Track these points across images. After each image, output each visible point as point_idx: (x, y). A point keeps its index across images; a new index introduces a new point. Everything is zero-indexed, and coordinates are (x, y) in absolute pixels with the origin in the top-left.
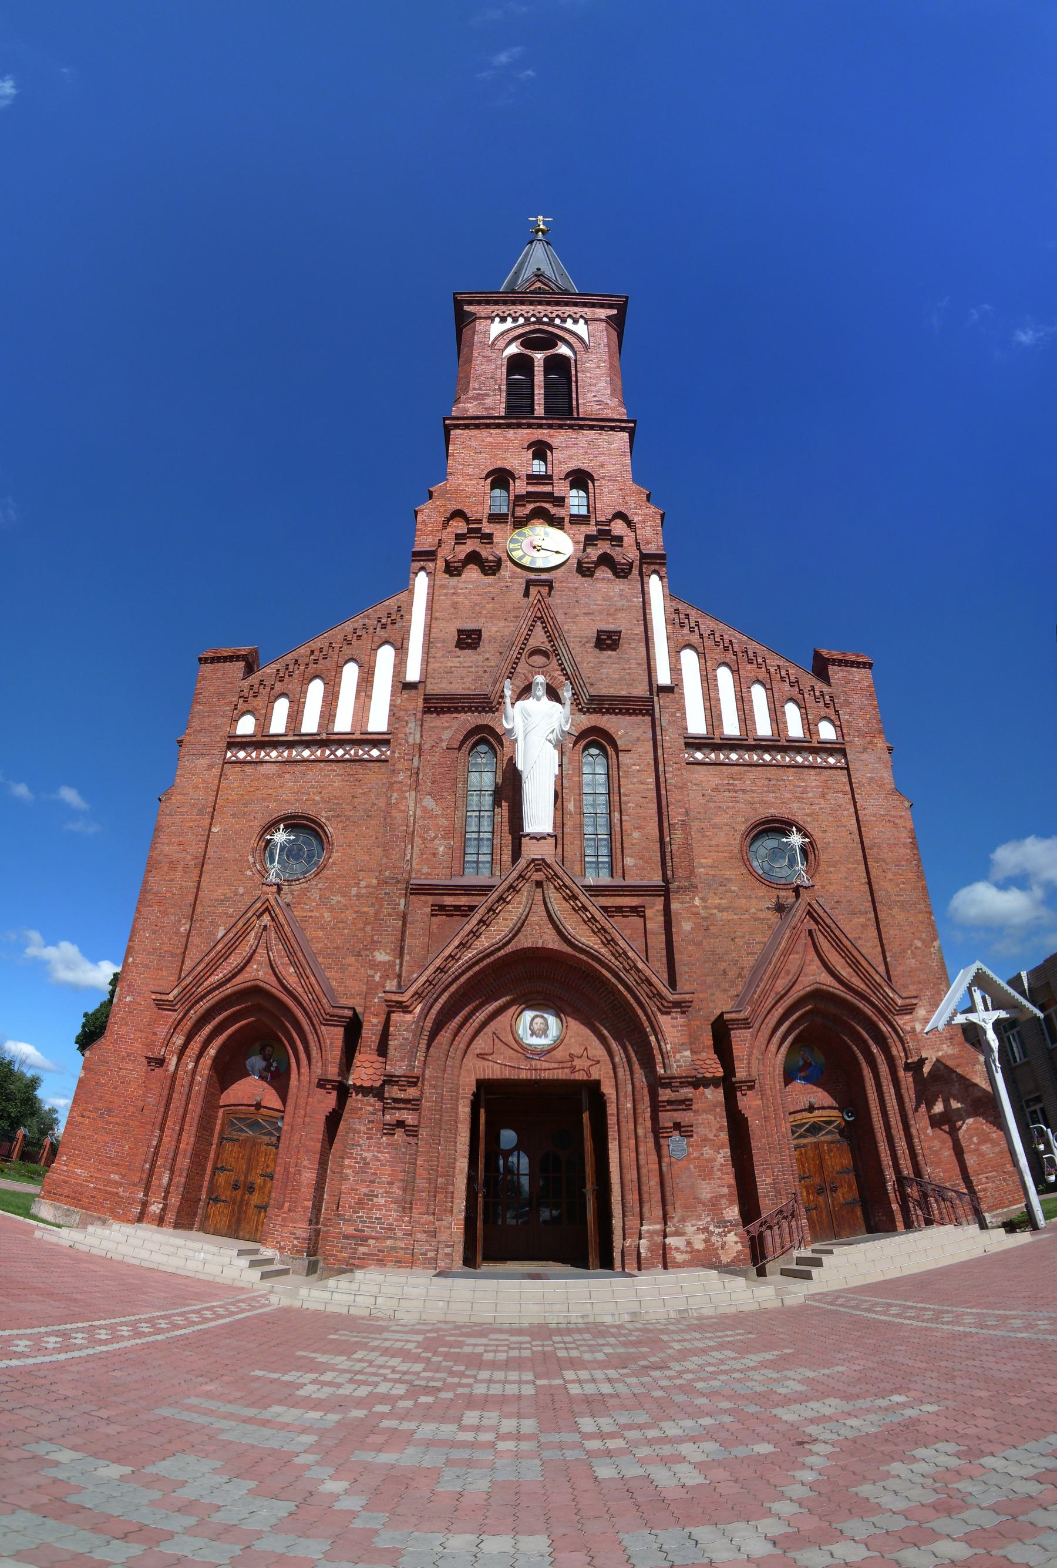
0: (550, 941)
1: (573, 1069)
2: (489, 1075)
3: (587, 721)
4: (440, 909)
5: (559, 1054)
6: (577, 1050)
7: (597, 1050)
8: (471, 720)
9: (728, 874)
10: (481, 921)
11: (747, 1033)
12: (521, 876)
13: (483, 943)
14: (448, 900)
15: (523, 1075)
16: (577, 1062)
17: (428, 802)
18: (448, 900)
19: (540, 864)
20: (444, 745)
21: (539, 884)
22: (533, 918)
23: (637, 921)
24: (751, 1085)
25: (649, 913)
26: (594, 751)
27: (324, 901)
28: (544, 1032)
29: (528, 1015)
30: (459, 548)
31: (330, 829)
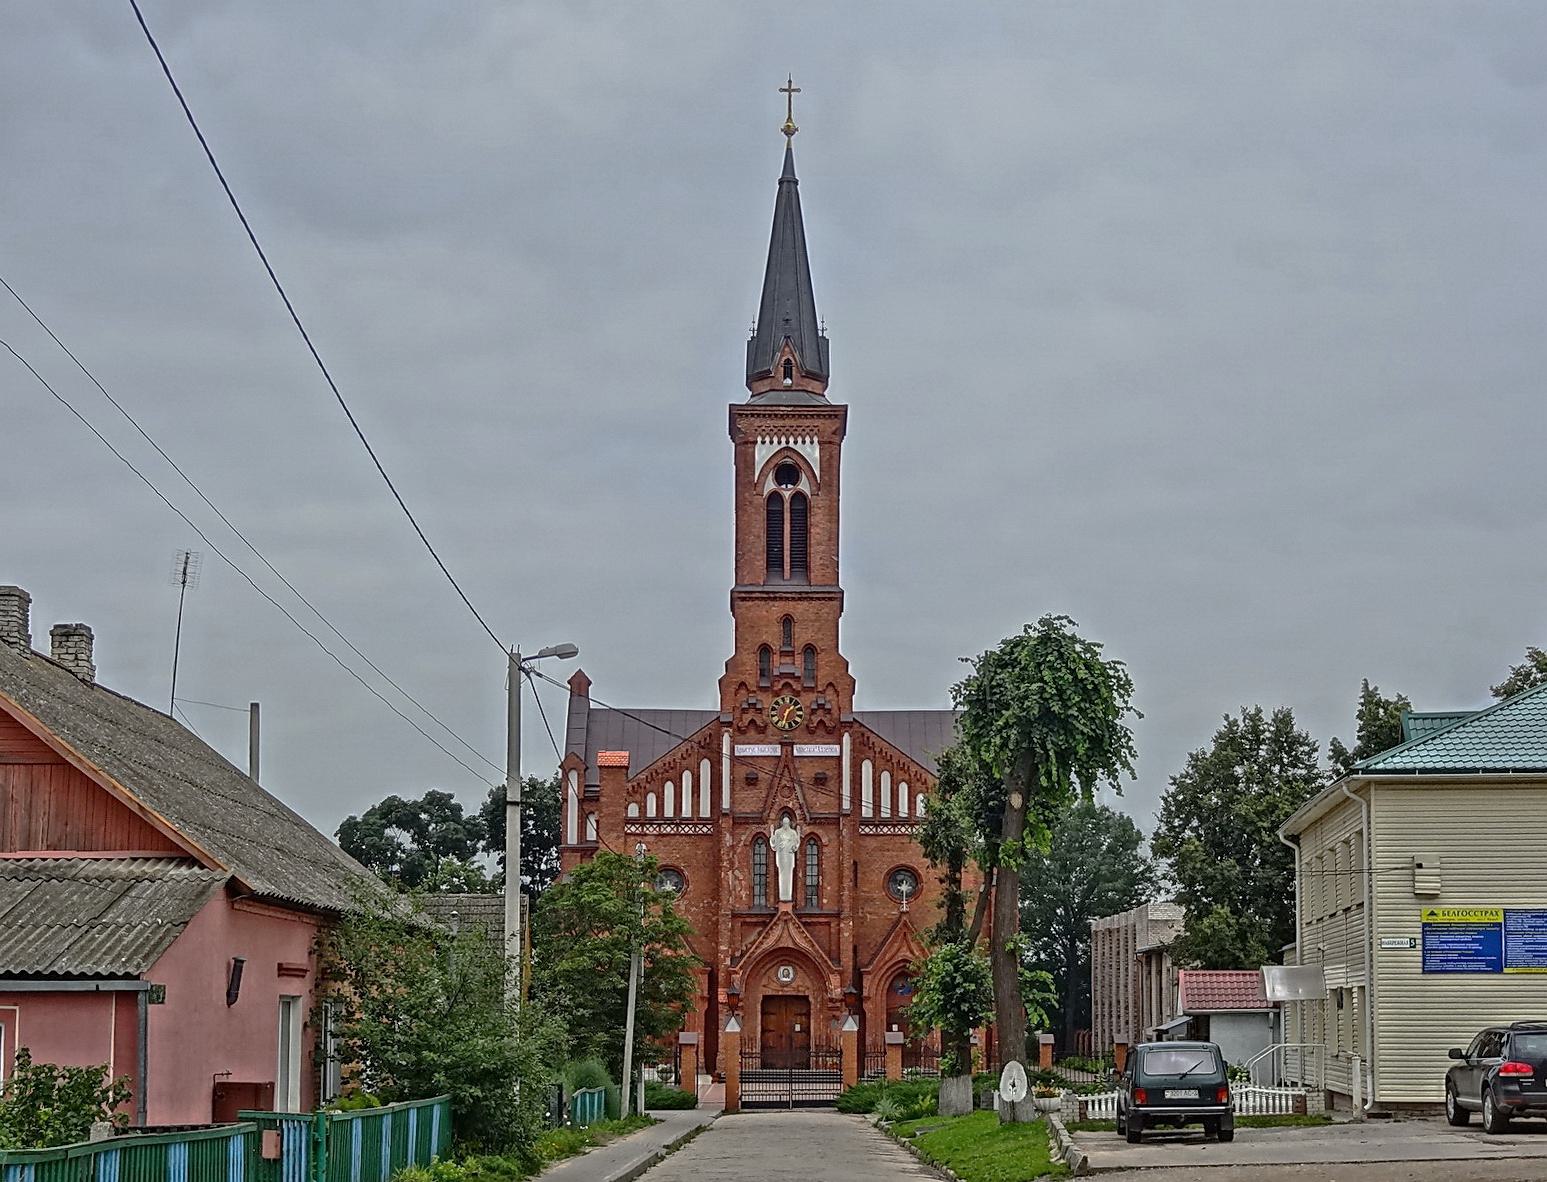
0: (791, 946)
1: (799, 991)
2: (767, 994)
3: (808, 829)
4: (744, 924)
5: (793, 984)
6: (801, 984)
7: (808, 984)
8: (755, 829)
9: (875, 896)
10: (764, 938)
11: (870, 977)
12: (779, 919)
13: (764, 946)
14: (748, 920)
15: (780, 993)
16: (800, 988)
17: (737, 872)
18: (748, 920)
19: (787, 913)
20: (742, 843)
21: (786, 921)
22: (784, 935)
23: (827, 927)
24: (869, 998)
25: (832, 925)
26: (812, 842)
27: (687, 911)
28: (788, 976)
29: (782, 968)
30: (745, 716)
31: (686, 873)
